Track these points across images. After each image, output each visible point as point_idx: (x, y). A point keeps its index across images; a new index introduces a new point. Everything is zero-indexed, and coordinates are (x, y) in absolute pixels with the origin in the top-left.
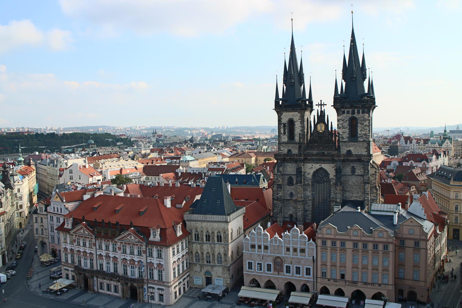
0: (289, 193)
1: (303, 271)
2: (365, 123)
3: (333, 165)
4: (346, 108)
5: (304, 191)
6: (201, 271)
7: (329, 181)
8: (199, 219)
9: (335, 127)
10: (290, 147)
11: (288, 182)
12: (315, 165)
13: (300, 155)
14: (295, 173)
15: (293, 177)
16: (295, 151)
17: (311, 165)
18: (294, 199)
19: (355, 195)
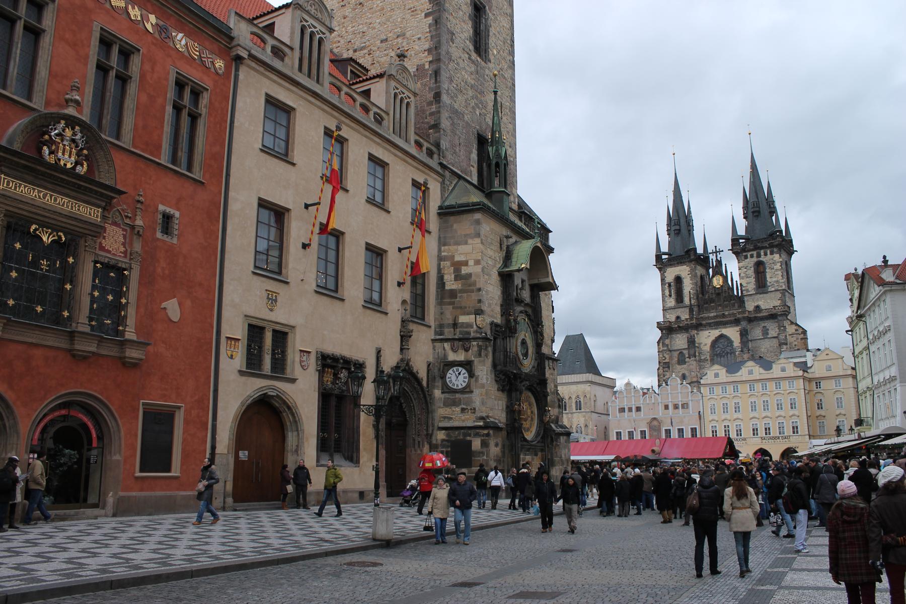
2: (775, 267)
3: (738, 328)
4: (749, 251)
5: (700, 369)
7: (733, 352)
9: (736, 278)
13: (691, 318)
16: (685, 315)
17: (707, 332)
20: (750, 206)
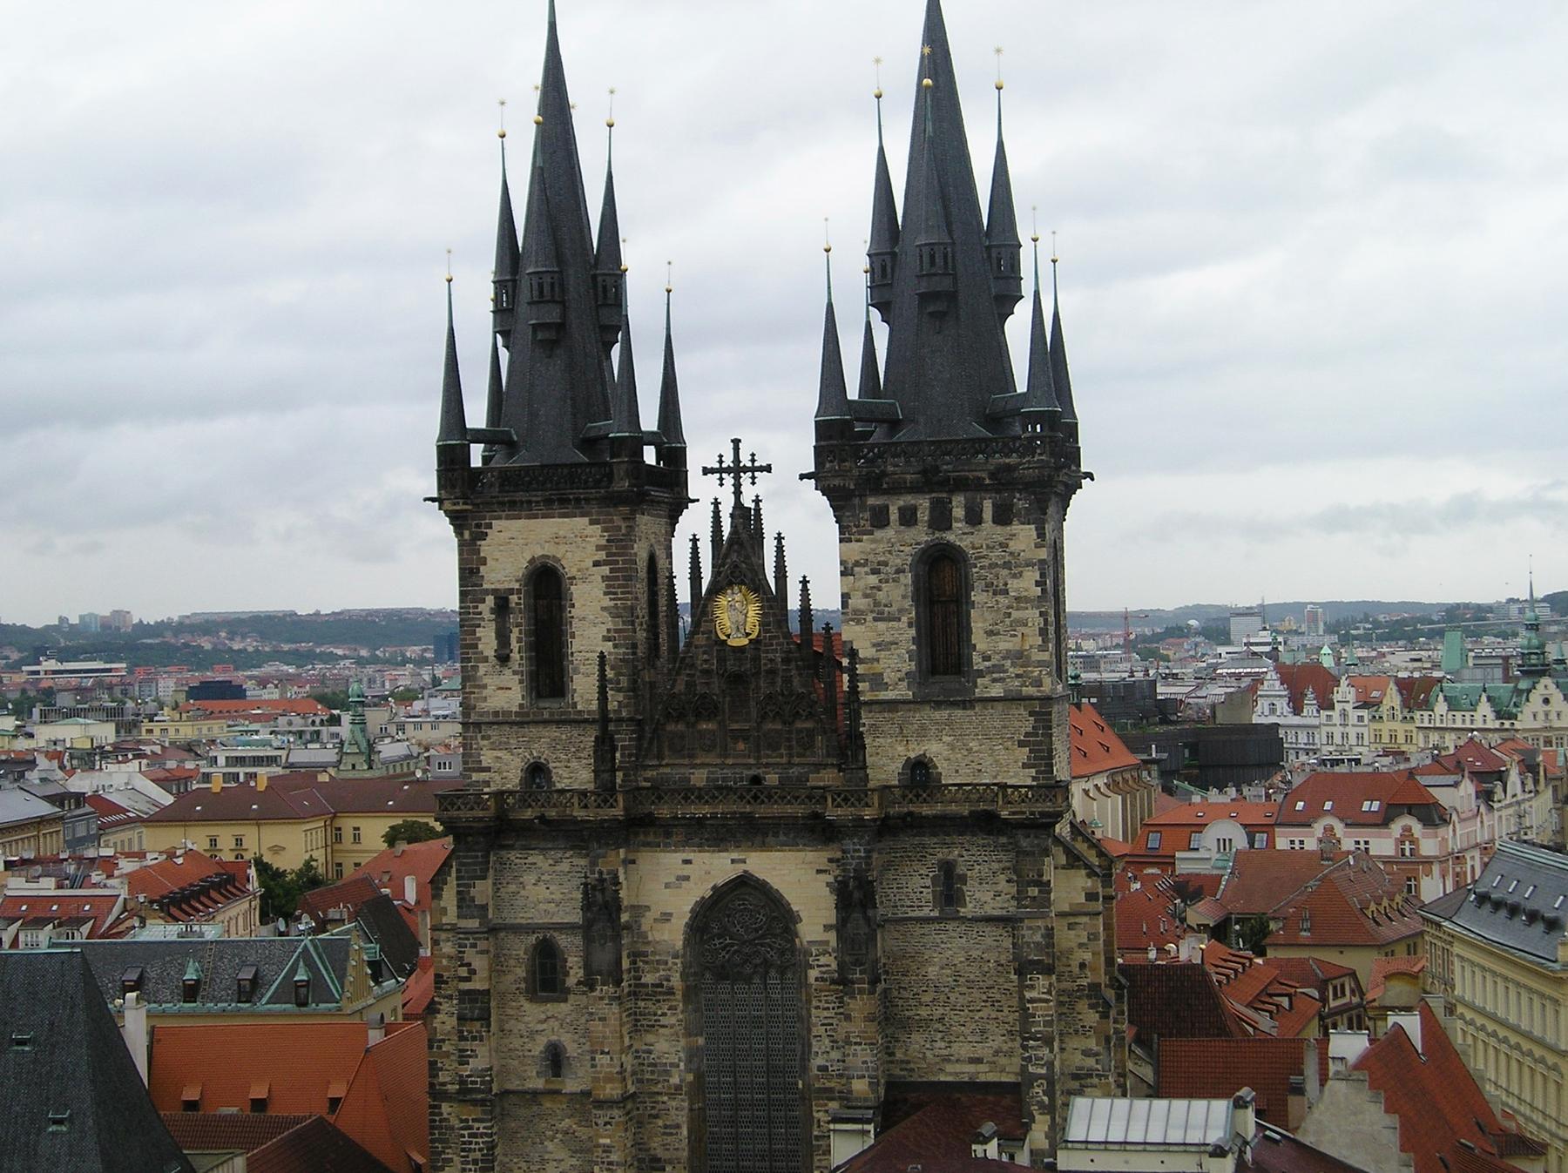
0: (538, 1047)
2: (1013, 584)
3: (817, 857)
4: (897, 489)
5: (636, 1030)
10: (542, 744)
11: (531, 972)
13: (606, 791)
14: (576, 917)
15: (563, 940)
16: (574, 772)
18: (571, 1085)
19: (962, 1050)
20: (910, 263)
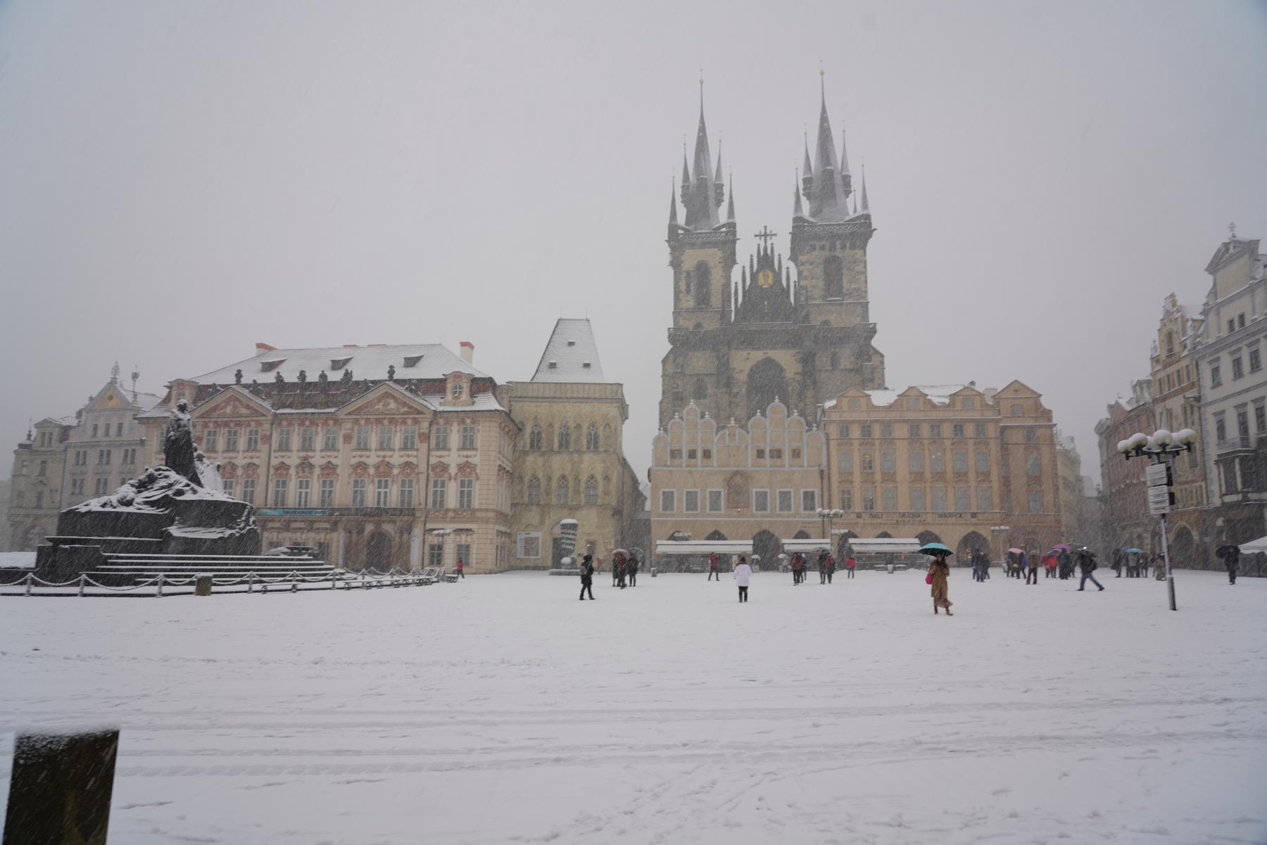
1: (797, 501)
6: (542, 523)
8: (547, 395)
9: (794, 277)
12: (752, 353)
